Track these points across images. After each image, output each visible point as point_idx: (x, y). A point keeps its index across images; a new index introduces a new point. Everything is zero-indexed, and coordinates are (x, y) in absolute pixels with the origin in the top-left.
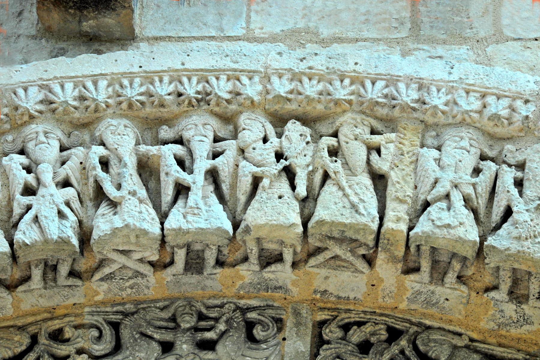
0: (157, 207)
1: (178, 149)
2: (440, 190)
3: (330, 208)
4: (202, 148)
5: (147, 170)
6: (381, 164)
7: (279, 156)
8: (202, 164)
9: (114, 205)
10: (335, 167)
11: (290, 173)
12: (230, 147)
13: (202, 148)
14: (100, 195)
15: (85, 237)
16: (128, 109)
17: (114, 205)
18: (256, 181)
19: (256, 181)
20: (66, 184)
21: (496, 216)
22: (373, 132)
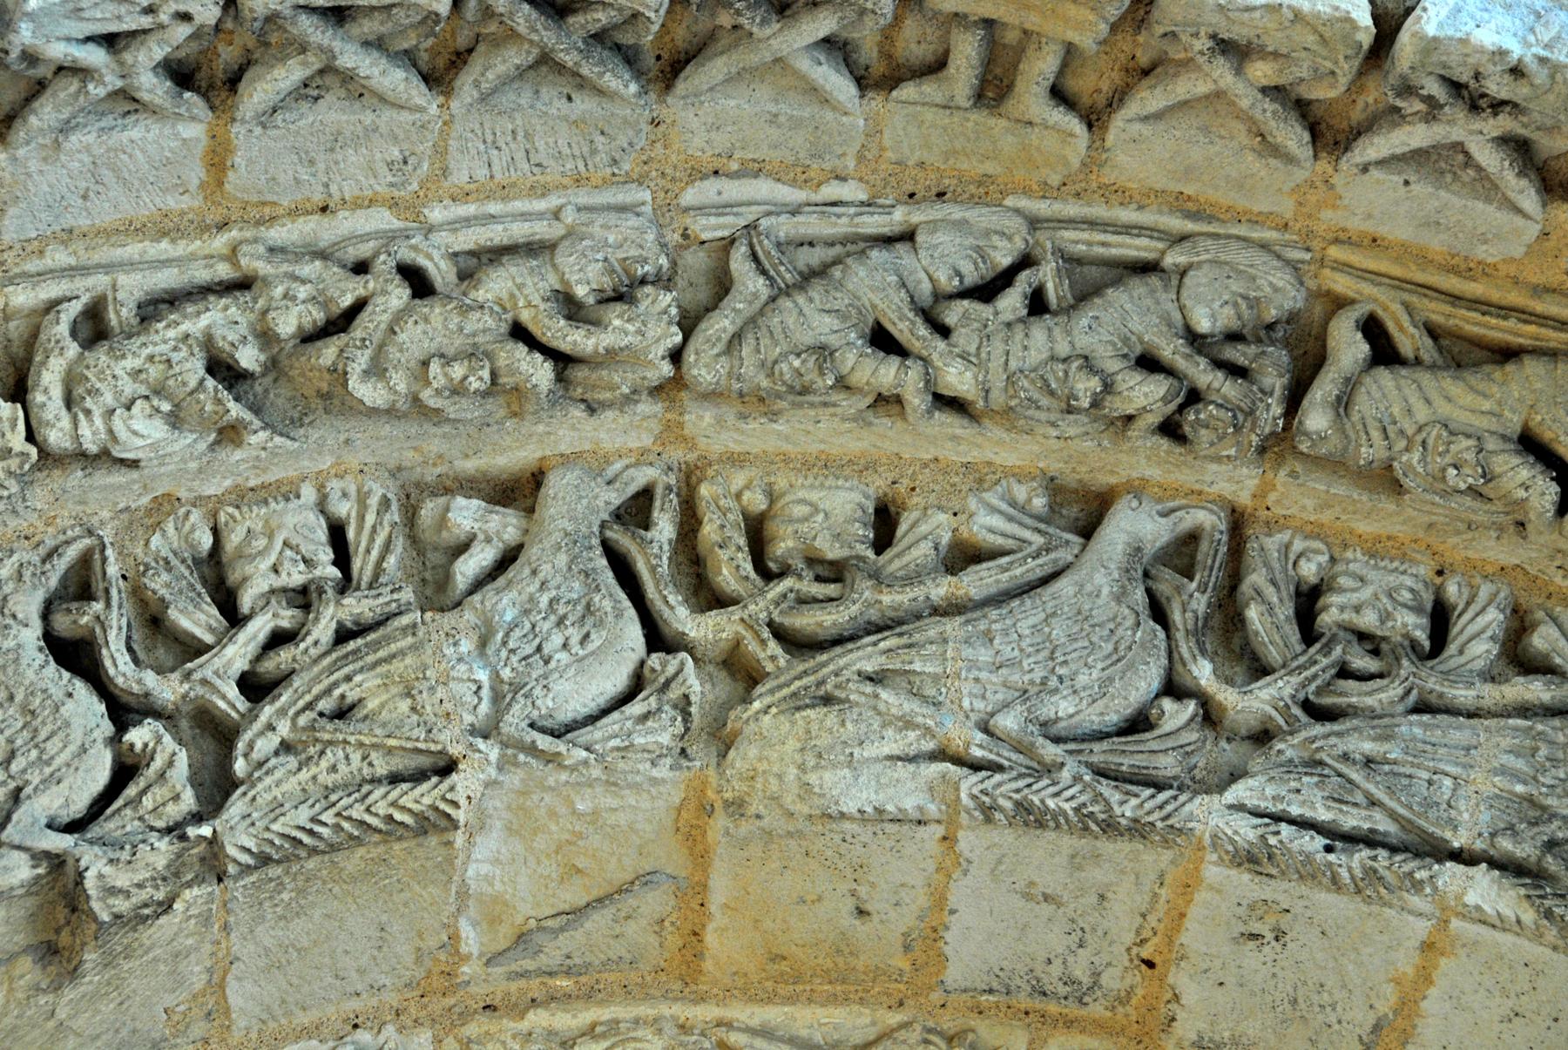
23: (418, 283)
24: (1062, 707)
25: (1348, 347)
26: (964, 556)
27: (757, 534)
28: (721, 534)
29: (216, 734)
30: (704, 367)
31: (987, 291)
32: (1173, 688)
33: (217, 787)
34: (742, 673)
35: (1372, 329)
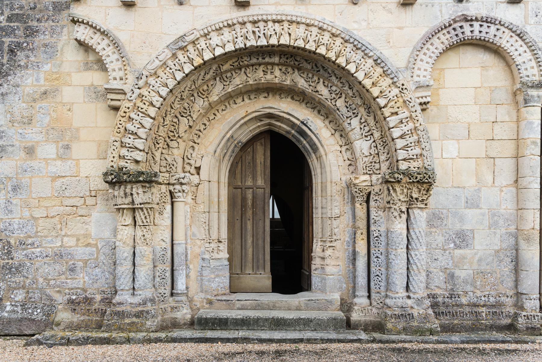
0: (256, 39)
1: (258, 29)
2: (299, 37)
3: (282, 42)
4: (262, 28)
5: (254, 32)
6: (290, 32)
7: (274, 30)
8: (262, 32)
9: (249, 40)
10: (283, 33)
11: (276, 33)
12: (266, 28)
13: (262, 28)
14: (247, 38)
15: (245, 45)
16: (250, 22)
17: (249, 40)
18: (271, 35)
19: (271, 35)
20: (242, 36)
21: (307, 41)
22: (289, 25)
23: (183, 92)
24: (221, 90)
25: (221, 66)
26: (212, 85)
27: (203, 90)
28: (202, 91)
29: (190, 115)
30: (197, 86)
31: (205, 74)
32: (224, 85)
33: (192, 118)
34: (207, 97)
35: (221, 65)
